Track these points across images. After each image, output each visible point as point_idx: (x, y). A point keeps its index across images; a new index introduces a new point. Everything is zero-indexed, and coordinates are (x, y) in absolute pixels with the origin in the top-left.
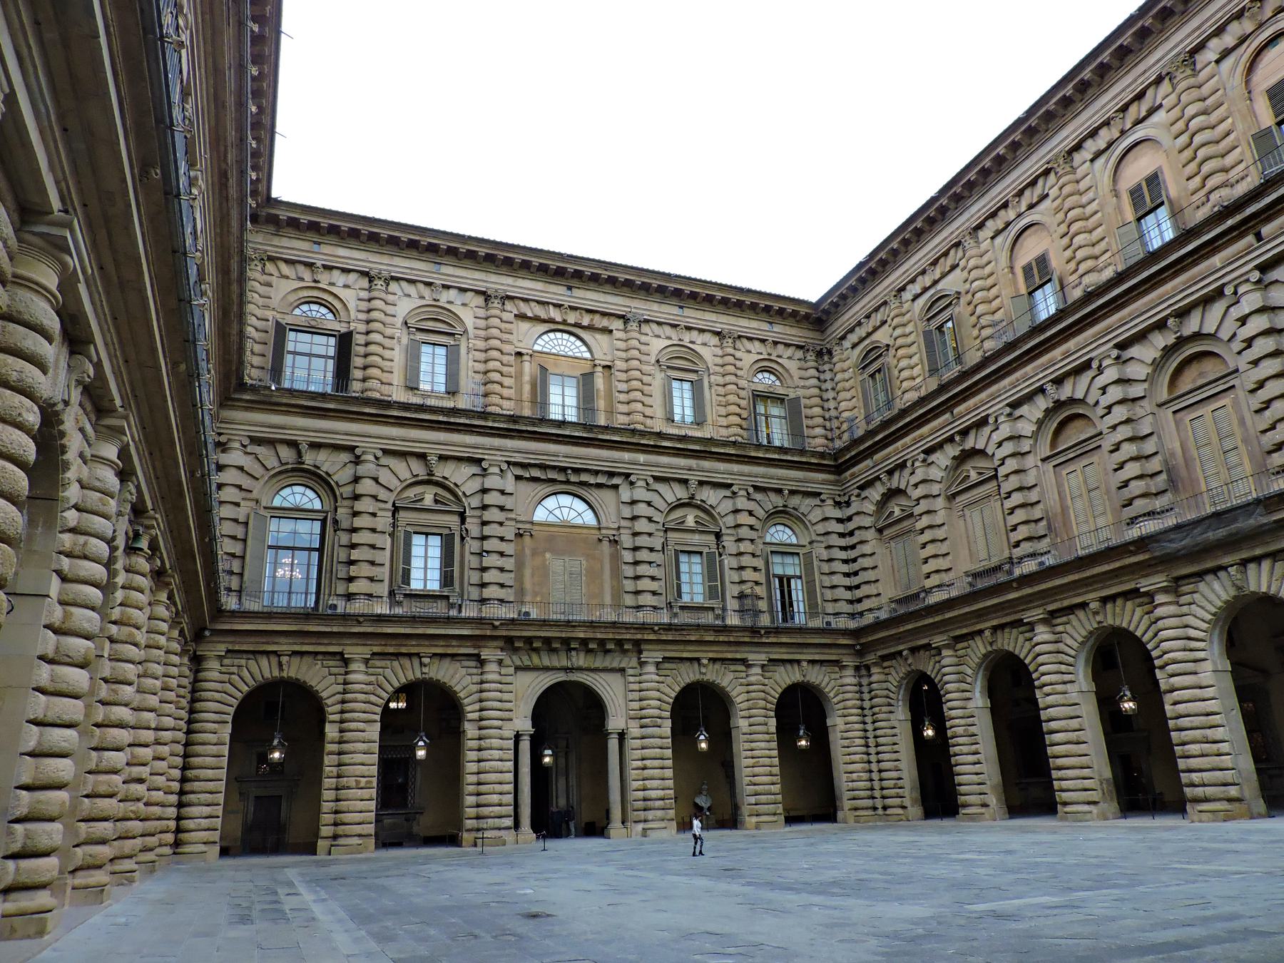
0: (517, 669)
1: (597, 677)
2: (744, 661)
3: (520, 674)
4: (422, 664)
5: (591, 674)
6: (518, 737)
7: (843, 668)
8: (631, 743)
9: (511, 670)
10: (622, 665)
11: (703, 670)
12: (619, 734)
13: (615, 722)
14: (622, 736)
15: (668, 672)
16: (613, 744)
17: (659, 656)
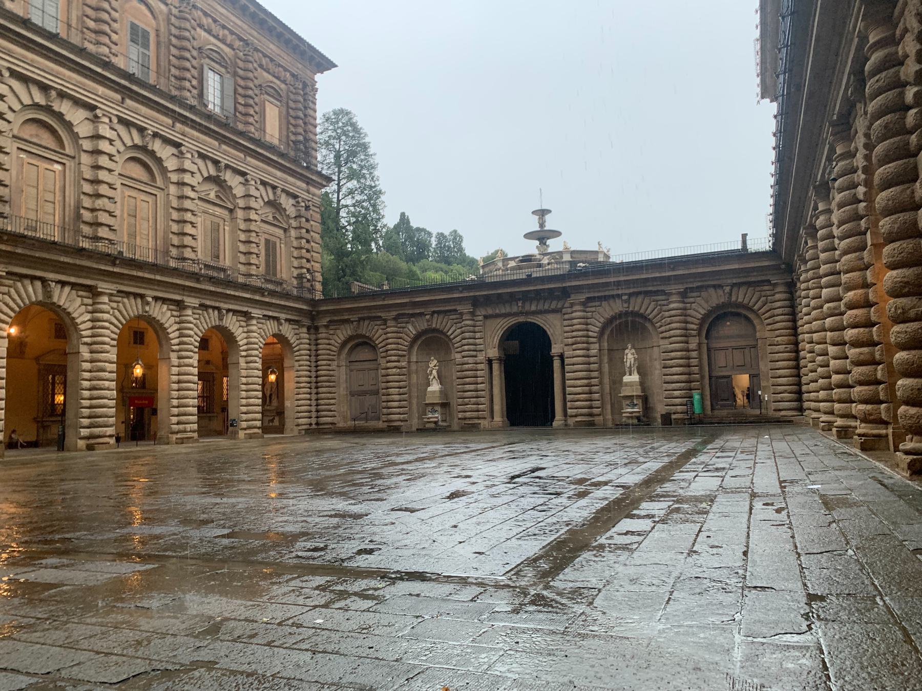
0: (486, 317)
1: (544, 318)
2: (663, 292)
3: (488, 322)
4: (428, 321)
5: (539, 316)
6: (490, 362)
7: (775, 285)
8: (567, 361)
9: (481, 318)
10: (559, 306)
11: (626, 305)
12: (558, 356)
13: (556, 350)
14: (562, 357)
15: (593, 309)
16: (557, 364)
17: (582, 297)
